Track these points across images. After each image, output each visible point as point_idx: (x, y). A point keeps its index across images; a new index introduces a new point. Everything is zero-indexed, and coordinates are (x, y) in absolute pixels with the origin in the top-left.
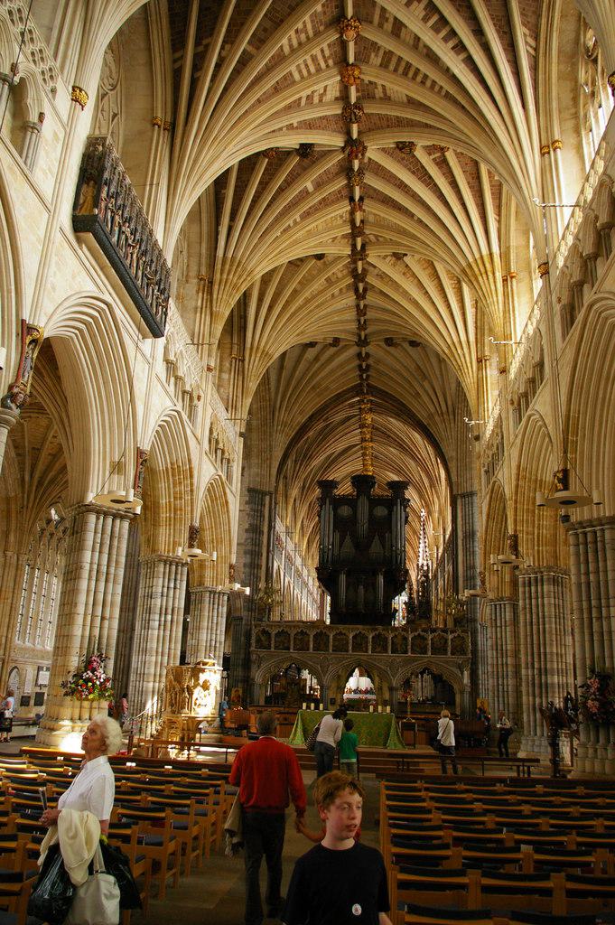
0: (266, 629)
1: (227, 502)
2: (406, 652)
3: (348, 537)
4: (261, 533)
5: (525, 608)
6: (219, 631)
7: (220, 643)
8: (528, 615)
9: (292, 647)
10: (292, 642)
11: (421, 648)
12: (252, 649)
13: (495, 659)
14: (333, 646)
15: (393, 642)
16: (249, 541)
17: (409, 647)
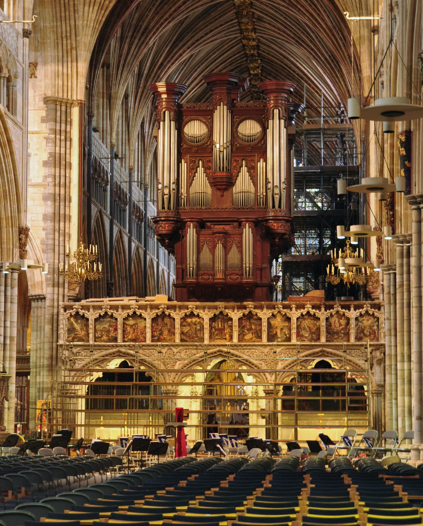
0: (81, 312)
1: (9, 141)
2: (289, 339)
3: (201, 170)
4: (68, 166)
5: (402, 285)
6: (8, 324)
7: (11, 338)
8: (405, 294)
9: (120, 337)
10: (120, 331)
11: (311, 333)
12: (61, 342)
13: (393, 348)
14: (182, 333)
15: (269, 324)
16: (50, 180)
17: (294, 331)
